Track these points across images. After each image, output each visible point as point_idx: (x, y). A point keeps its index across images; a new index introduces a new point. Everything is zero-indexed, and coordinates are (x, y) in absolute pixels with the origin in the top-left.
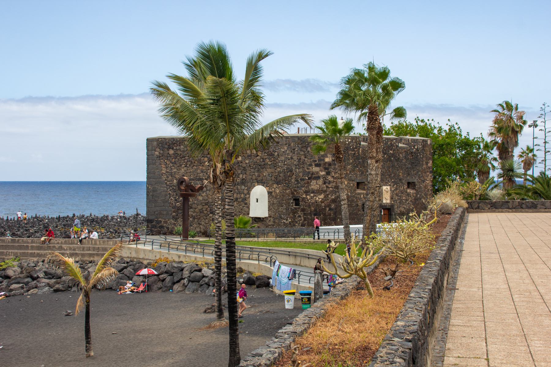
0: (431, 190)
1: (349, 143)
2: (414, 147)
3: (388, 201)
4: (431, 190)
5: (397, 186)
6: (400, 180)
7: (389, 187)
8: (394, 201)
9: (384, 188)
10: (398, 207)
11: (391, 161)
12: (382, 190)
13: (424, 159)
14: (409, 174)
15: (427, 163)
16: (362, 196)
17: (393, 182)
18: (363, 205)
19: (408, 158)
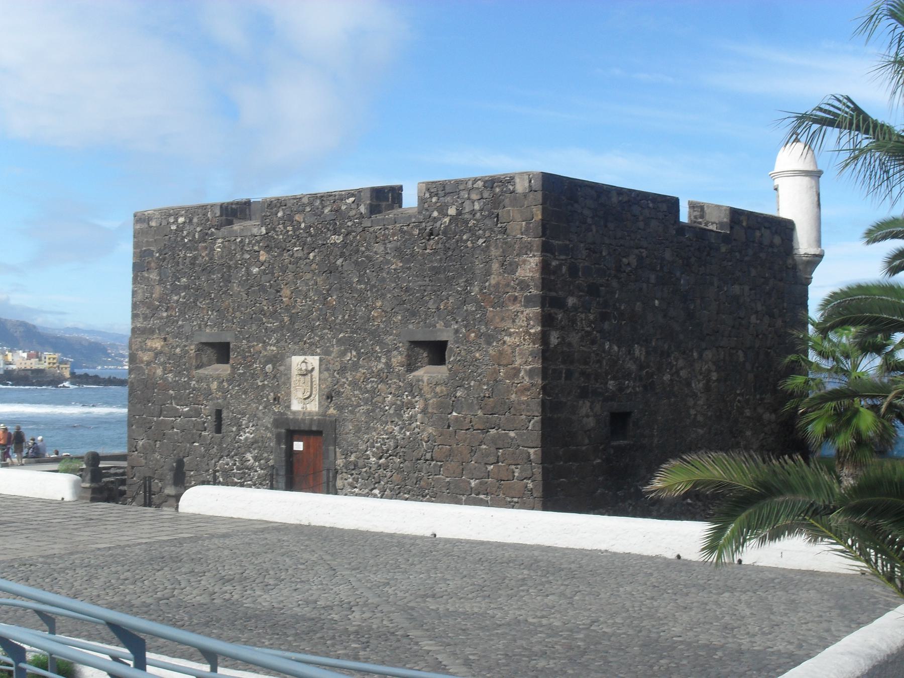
0: (531, 373)
1: (180, 229)
2: (443, 212)
3: (313, 407)
4: (531, 373)
5: (359, 355)
6: (375, 334)
7: (314, 361)
8: (340, 408)
9: (296, 361)
10: (358, 430)
11: (331, 270)
12: (289, 368)
13: (494, 252)
14: (414, 314)
15: (510, 268)
16: (214, 385)
17: (340, 342)
18: (219, 413)
19: (413, 255)
